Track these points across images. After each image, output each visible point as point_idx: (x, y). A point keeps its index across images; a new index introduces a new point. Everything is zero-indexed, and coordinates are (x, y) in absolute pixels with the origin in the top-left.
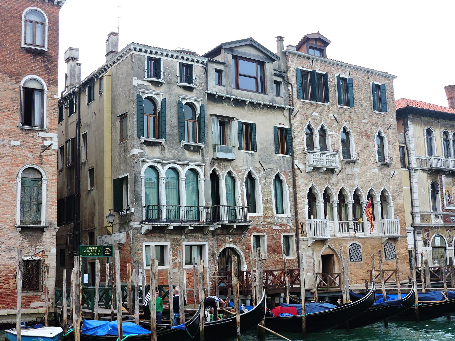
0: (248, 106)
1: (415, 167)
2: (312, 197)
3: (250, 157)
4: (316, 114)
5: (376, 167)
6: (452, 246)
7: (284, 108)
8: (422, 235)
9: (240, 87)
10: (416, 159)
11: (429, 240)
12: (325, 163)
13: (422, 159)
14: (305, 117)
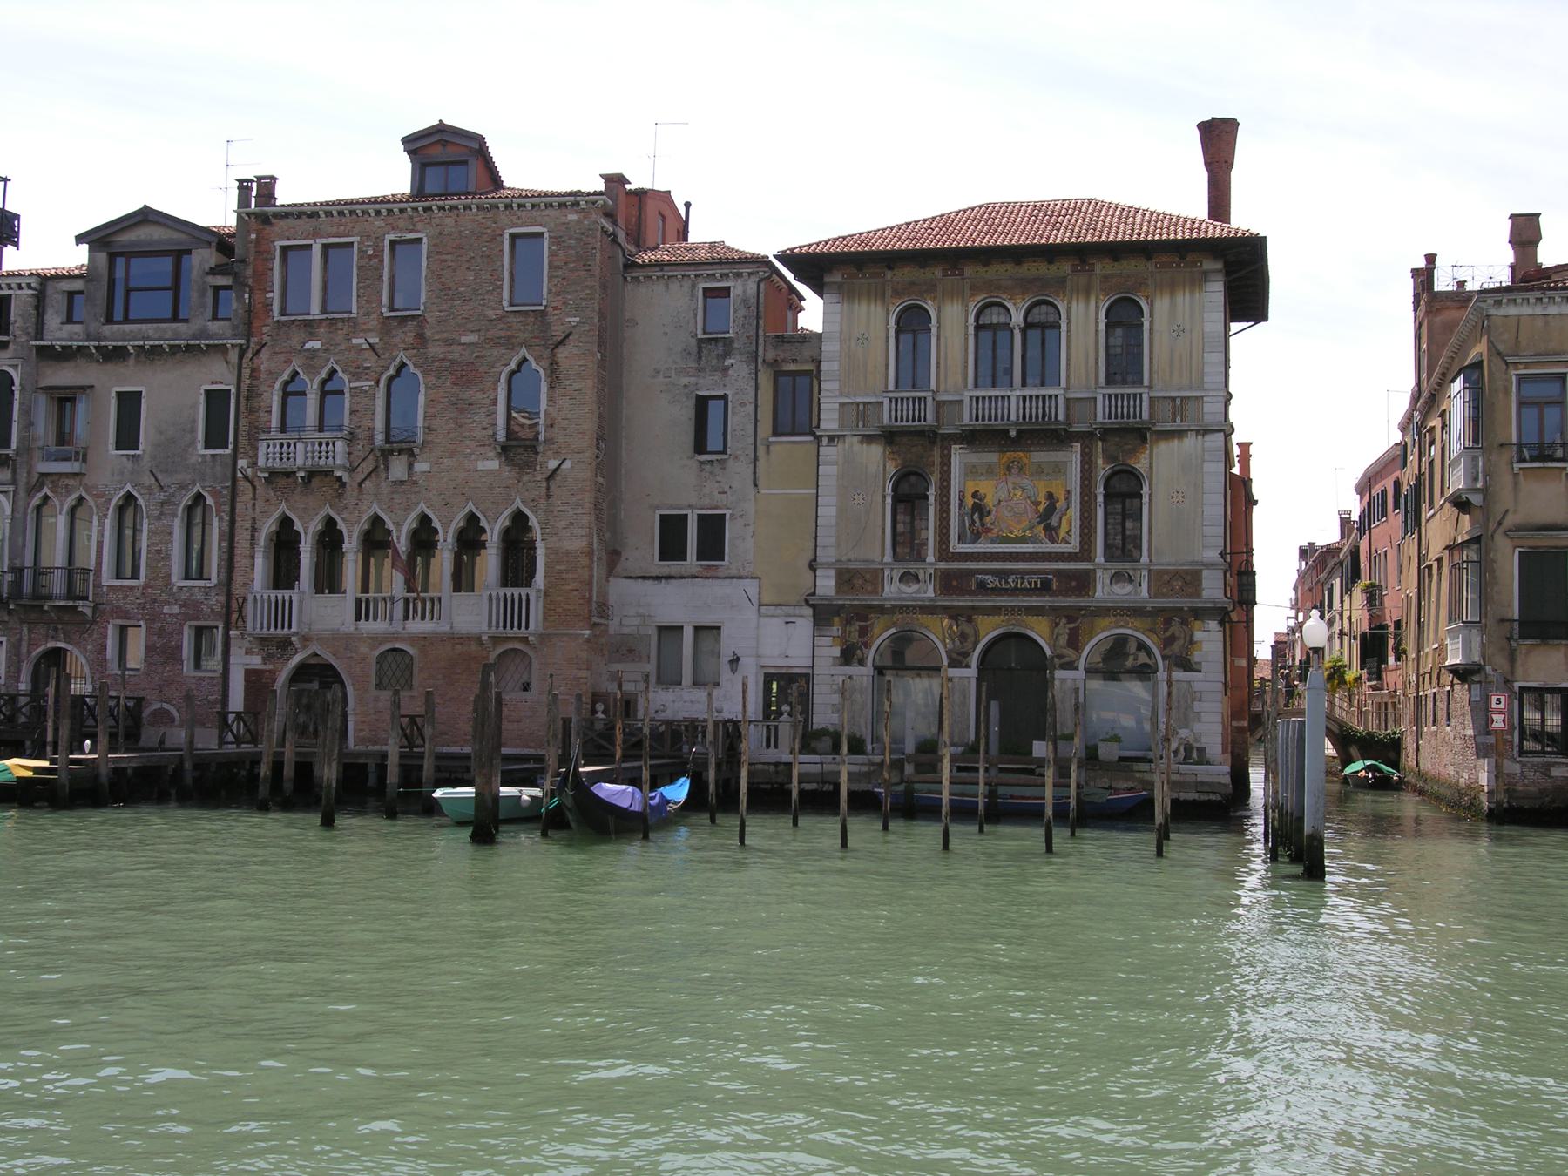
0: (138, 355)
1: (835, 430)
2: (285, 541)
3: (129, 465)
4: (317, 345)
5: (492, 454)
6: (968, 666)
7: (225, 345)
8: (835, 630)
9: (131, 317)
10: (843, 405)
11: (867, 645)
12: (300, 462)
13: (865, 404)
14: (282, 358)
